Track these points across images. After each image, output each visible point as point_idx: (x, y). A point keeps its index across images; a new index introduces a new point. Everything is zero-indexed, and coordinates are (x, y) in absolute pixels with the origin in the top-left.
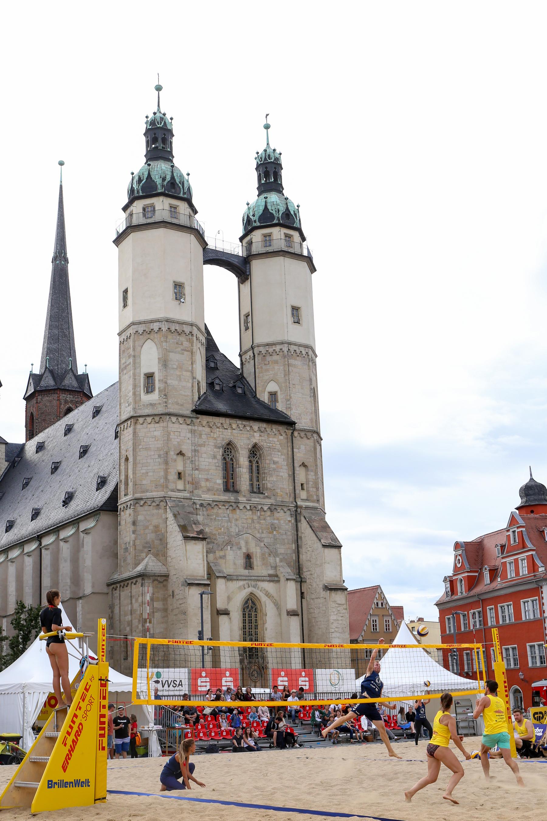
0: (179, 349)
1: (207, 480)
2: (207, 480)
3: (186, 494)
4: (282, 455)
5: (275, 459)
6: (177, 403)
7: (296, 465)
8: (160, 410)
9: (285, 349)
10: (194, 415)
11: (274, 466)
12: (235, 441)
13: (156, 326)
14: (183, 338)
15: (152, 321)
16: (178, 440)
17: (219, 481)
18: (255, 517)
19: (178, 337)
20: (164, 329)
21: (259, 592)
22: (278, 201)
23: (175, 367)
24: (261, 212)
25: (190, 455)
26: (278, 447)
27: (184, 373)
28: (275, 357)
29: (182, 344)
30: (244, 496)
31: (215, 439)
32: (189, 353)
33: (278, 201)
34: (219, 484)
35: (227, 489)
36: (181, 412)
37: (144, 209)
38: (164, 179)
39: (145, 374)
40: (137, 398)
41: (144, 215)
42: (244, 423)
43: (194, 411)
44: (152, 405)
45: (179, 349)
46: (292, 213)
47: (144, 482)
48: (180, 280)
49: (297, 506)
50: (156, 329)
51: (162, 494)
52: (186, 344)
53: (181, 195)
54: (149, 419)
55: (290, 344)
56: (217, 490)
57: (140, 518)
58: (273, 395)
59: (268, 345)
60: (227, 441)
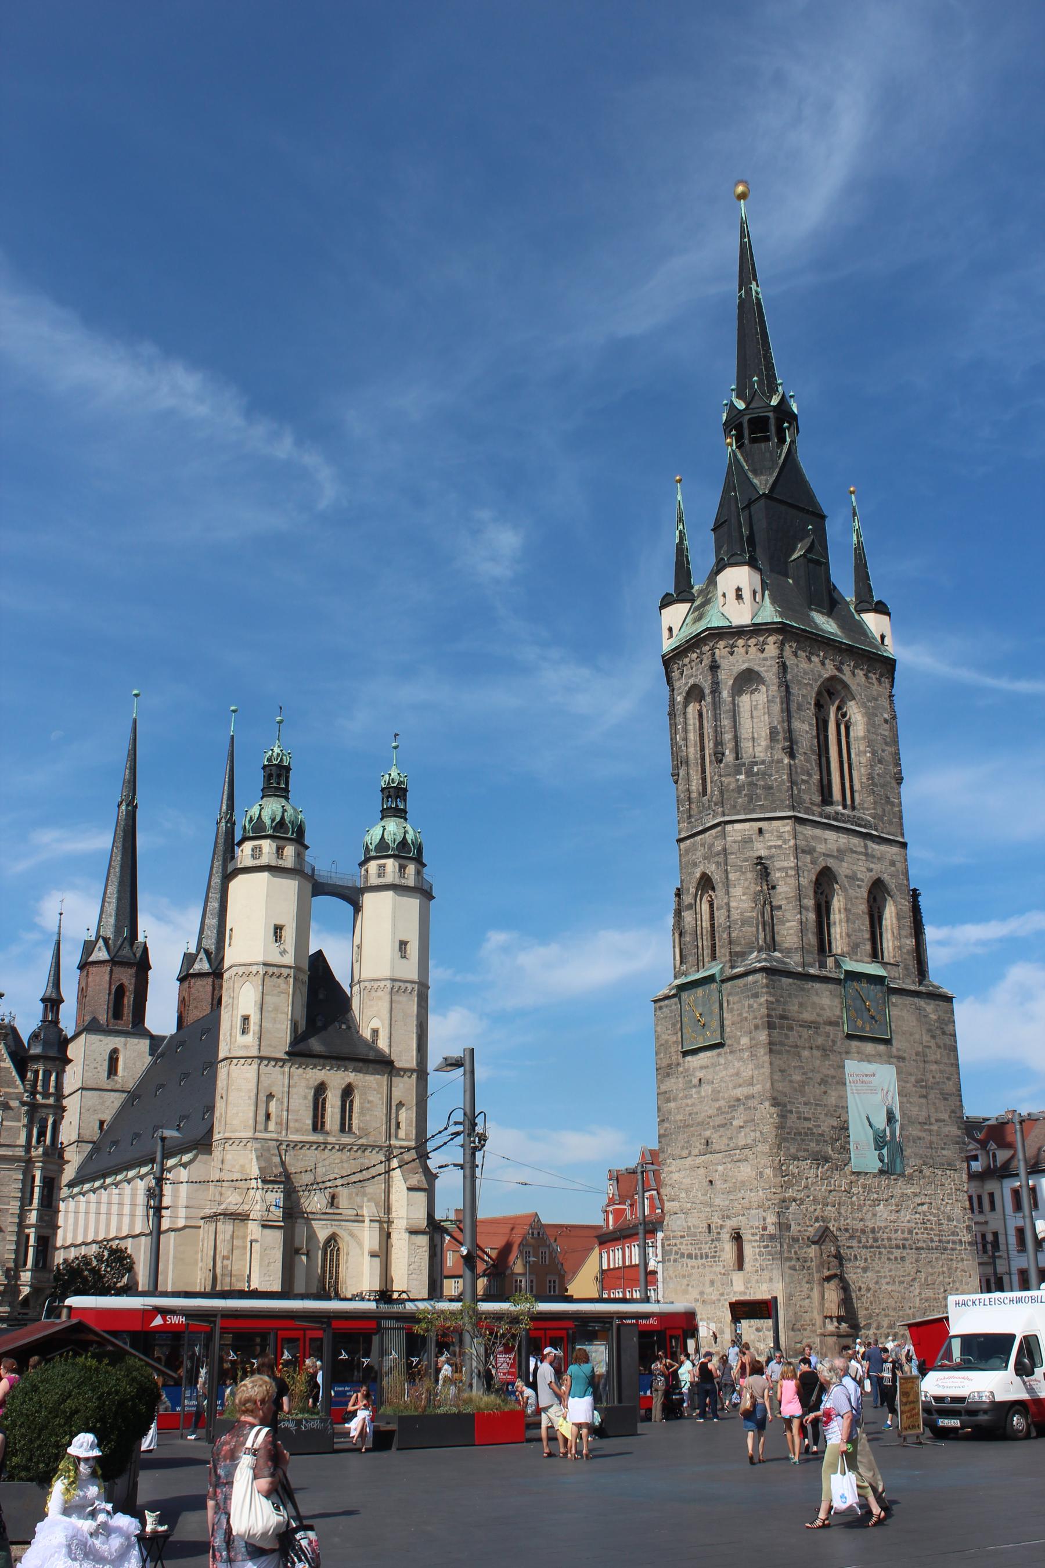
0: (275, 992)
1: (296, 1121)
2: (296, 1121)
3: (274, 1136)
4: (378, 1093)
5: (371, 1098)
6: (270, 1045)
7: (394, 1104)
8: (255, 1053)
9: (389, 984)
10: (287, 1057)
11: (368, 1105)
12: (328, 1081)
13: (254, 969)
14: (281, 980)
15: (251, 965)
16: (269, 1082)
17: (309, 1122)
18: (344, 1157)
19: (276, 980)
20: (261, 973)
21: (342, 1231)
22: (396, 830)
23: (270, 1009)
24: (378, 840)
25: (280, 1096)
26: (375, 1086)
27: (279, 1015)
28: (380, 993)
29: (279, 987)
30: (334, 1136)
31: (307, 1080)
32: (286, 996)
33: (396, 830)
34: (308, 1125)
35: (315, 1129)
36: (274, 1055)
37: (253, 850)
38: (273, 820)
39: (242, 1016)
40: (233, 1039)
41: (254, 857)
42: (339, 1063)
43: (287, 1053)
44: (246, 1047)
45: (275, 992)
46: (410, 841)
47: (234, 1122)
48: (280, 922)
49: (390, 1146)
50: (254, 972)
51: (250, 1134)
52: (283, 986)
53: (289, 835)
54: (242, 1061)
55: (393, 980)
56: (306, 1130)
57: (229, 1157)
58: (375, 1032)
59: (373, 980)
60: (319, 1082)
